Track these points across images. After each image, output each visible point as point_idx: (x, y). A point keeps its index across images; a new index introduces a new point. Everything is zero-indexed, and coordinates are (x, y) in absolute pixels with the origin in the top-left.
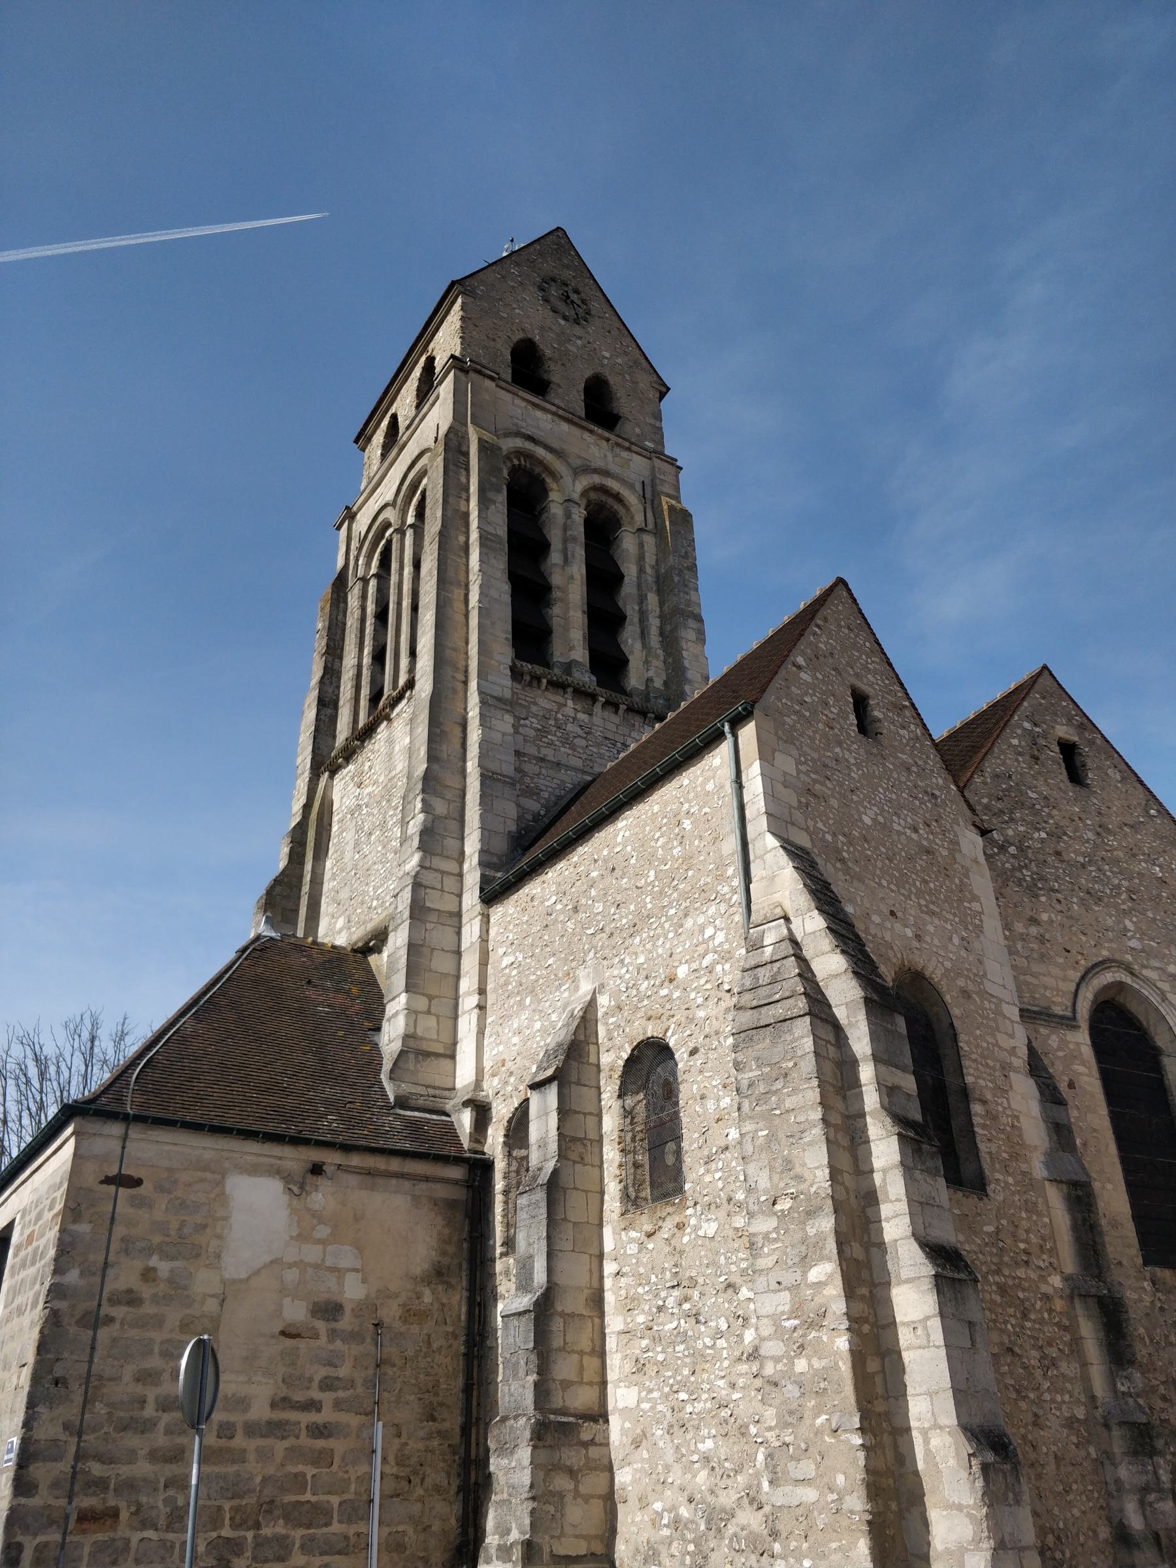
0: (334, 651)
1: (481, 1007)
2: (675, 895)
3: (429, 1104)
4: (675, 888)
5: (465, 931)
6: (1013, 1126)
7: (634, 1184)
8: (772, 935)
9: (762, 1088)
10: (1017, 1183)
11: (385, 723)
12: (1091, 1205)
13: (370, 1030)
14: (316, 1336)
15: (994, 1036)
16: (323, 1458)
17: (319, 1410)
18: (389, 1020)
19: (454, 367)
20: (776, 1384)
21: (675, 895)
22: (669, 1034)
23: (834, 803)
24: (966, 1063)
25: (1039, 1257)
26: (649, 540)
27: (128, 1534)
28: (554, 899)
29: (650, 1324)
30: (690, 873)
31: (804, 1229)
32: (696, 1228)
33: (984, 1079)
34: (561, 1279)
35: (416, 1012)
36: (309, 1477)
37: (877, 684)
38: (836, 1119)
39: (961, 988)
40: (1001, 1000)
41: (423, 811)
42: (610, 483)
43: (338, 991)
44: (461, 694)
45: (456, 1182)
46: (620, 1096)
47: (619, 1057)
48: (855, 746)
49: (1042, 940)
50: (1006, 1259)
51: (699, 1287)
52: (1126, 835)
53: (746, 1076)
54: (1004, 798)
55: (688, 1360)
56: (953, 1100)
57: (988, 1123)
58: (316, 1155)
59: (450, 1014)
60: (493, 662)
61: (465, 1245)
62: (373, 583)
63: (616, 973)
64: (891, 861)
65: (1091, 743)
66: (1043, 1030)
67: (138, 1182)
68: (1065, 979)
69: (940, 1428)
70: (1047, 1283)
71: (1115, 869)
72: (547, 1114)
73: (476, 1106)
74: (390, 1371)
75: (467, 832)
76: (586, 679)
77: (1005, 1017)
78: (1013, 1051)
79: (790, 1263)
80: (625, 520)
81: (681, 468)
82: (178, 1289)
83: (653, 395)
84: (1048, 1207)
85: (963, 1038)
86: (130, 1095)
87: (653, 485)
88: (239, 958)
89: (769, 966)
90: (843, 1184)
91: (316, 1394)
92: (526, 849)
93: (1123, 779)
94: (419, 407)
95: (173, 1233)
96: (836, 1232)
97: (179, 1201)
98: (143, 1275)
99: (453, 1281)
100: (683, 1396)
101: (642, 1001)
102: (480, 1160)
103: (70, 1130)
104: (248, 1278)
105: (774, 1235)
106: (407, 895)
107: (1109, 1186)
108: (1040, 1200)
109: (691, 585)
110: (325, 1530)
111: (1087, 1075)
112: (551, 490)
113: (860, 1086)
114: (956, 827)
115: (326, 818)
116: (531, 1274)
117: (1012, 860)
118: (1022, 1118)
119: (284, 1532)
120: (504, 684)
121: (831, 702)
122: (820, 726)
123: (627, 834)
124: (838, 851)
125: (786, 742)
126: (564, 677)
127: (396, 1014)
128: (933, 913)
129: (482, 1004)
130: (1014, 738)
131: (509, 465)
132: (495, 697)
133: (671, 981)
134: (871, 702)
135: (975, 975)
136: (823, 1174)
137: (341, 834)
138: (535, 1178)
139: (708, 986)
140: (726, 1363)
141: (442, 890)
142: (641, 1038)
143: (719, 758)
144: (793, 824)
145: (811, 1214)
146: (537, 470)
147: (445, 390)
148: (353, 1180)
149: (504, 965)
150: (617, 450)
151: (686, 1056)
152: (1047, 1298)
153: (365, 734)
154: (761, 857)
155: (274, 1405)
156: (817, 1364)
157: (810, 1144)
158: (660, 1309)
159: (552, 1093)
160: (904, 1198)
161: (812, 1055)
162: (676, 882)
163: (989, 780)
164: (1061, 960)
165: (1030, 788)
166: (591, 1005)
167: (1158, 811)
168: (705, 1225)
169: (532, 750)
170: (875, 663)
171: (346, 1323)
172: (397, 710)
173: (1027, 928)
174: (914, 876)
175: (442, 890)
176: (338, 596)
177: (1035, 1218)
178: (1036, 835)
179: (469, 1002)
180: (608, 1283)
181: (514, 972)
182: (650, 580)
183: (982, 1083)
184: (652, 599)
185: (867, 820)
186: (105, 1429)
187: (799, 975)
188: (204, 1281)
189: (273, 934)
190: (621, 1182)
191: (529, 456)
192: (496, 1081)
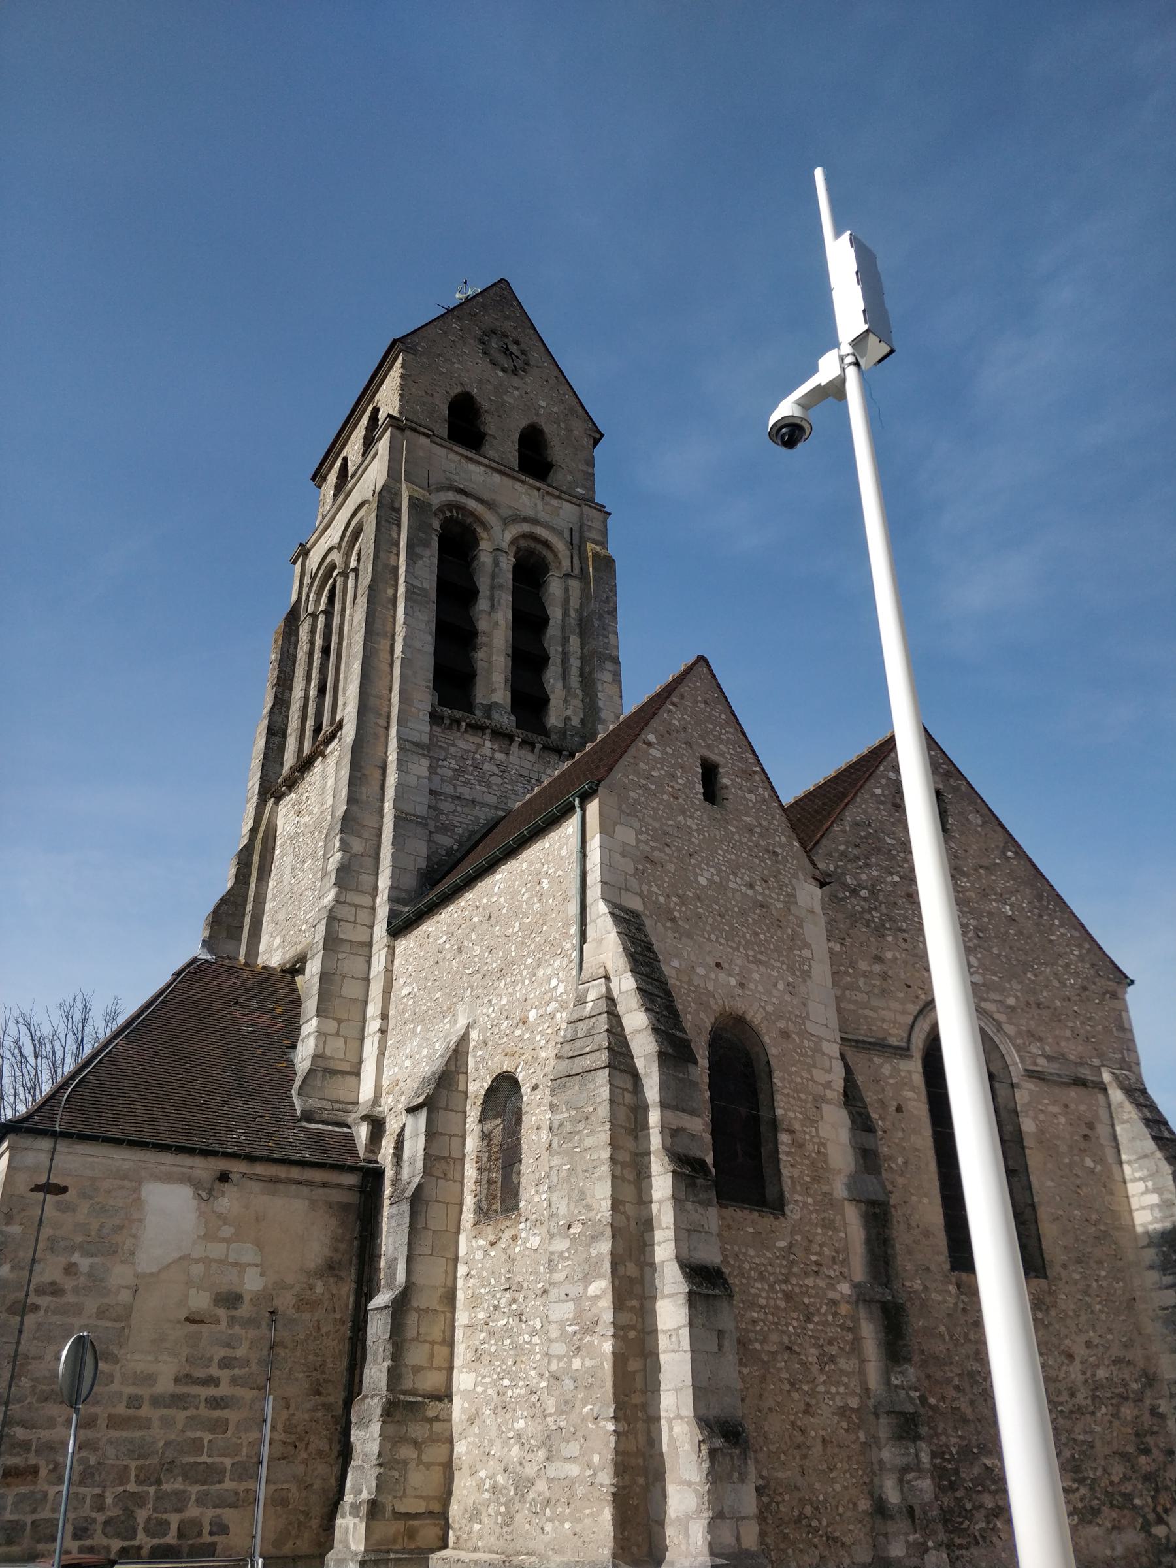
0: (284, 682)
1: (383, 1031)
2: (532, 946)
3: (333, 1118)
4: (533, 941)
5: (374, 959)
6: (819, 1152)
7: (487, 1198)
8: (595, 991)
9: (568, 1129)
10: (815, 1203)
11: (321, 758)
12: (886, 1221)
13: (288, 1047)
14: (217, 1322)
15: (810, 1072)
16: (219, 1426)
17: (217, 1385)
18: (303, 1040)
19: (391, 425)
20: (557, 1379)
21: (532, 946)
22: (519, 1070)
23: (671, 867)
24: (778, 1097)
25: (830, 1268)
26: (574, 585)
27: (46, 1487)
28: (445, 937)
29: (488, 1320)
30: (545, 928)
31: (588, 1251)
32: (526, 1241)
33: (794, 1111)
34: (418, 1279)
35: (325, 1035)
36: (206, 1442)
37: (729, 753)
38: (624, 1157)
39: (781, 1028)
40: (821, 1039)
41: (340, 849)
42: (540, 531)
43: (263, 1010)
44: (382, 739)
45: (350, 1188)
46: (480, 1121)
47: (482, 1087)
48: (699, 813)
49: (884, 976)
50: (795, 1270)
51: (524, 1292)
52: (979, 877)
53: (558, 1117)
54: (862, 845)
55: (511, 1352)
56: (763, 1129)
57: (793, 1150)
58: (223, 1165)
59: (357, 1035)
60: (413, 709)
61: (356, 1243)
62: (322, 618)
63: (485, 1011)
64: (722, 916)
65: (956, 790)
66: (877, 1060)
67: (64, 1190)
68: (904, 1012)
69: (682, 1418)
70: (835, 1290)
71: (965, 909)
72: (417, 1135)
73: (373, 1120)
74: (282, 1352)
75: (381, 868)
76: (505, 719)
77: (824, 1054)
78: (828, 1085)
79: (576, 1278)
80: (553, 565)
81: (610, 514)
82: (96, 1282)
83: (587, 442)
84: (845, 1223)
85: (777, 1074)
86: (60, 1113)
87: (581, 532)
88: (174, 981)
89: (587, 1020)
90: (624, 1213)
91: (214, 1371)
92: (434, 883)
93: (984, 823)
94: (365, 454)
95: (93, 1233)
96: (612, 1254)
97: (100, 1206)
98: (65, 1269)
99: (343, 1274)
100: (506, 1382)
101: (500, 1038)
102: (373, 1168)
103: (5, 1145)
104: (159, 1271)
105: (567, 1255)
106: (322, 927)
107: (925, 1200)
108: (838, 1217)
109: (610, 629)
110: (218, 1487)
111: (915, 1100)
112: (482, 539)
113: (648, 1128)
114: (794, 881)
115: (270, 839)
116: (395, 1274)
117: (863, 903)
118: (829, 1145)
119: (182, 1487)
120: (422, 729)
121: (679, 774)
122: (665, 797)
123: (502, 886)
124: (670, 911)
125: (628, 815)
126: (482, 720)
127: (308, 1036)
128: (760, 962)
129: (384, 1028)
130: (878, 788)
131: (441, 517)
132: (413, 743)
133: (524, 1023)
134: (721, 770)
135: (797, 1016)
136: (606, 1205)
137: (283, 858)
138: (404, 1191)
139: (549, 1031)
140: (538, 1357)
141: (355, 923)
142: (499, 1071)
143: (570, 828)
144: (627, 890)
145: (594, 1238)
146: (469, 521)
147: (383, 446)
148: (256, 1187)
149: (403, 995)
150: (548, 498)
151: (529, 1090)
152: (833, 1303)
153: (305, 765)
154: (595, 921)
155: (177, 1380)
156: (588, 1363)
157: (600, 1178)
158: (496, 1308)
159: (423, 1116)
160: (672, 1227)
161: (608, 1102)
162: (534, 935)
163: (848, 828)
164: (901, 995)
165: (888, 835)
166: (464, 1038)
167: (1016, 853)
168: (532, 1239)
169: (449, 789)
170: (729, 733)
171: (245, 1310)
172: (331, 747)
173: (870, 966)
174: (744, 929)
175: (355, 923)
176: (290, 629)
177: (830, 1233)
178: (889, 879)
179: (373, 1026)
180: (460, 1283)
181: (411, 1002)
182: (573, 622)
183: (791, 1114)
184: (575, 641)
185: (703, 881)
186: (29, 1400)
187: (607, 1030)
188: (119, 1275)
189: (208, 957)
190: (475, 1196)
191: (461, 508)
192: (391, 1098)
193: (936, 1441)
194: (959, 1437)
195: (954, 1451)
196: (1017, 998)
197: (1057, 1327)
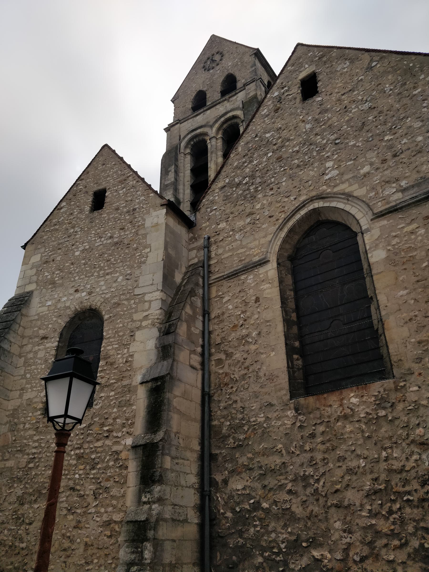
193: (265, 538)
194: (289, 533)
195: (283, 546)
196: (371, 164)
197: (405, 419)
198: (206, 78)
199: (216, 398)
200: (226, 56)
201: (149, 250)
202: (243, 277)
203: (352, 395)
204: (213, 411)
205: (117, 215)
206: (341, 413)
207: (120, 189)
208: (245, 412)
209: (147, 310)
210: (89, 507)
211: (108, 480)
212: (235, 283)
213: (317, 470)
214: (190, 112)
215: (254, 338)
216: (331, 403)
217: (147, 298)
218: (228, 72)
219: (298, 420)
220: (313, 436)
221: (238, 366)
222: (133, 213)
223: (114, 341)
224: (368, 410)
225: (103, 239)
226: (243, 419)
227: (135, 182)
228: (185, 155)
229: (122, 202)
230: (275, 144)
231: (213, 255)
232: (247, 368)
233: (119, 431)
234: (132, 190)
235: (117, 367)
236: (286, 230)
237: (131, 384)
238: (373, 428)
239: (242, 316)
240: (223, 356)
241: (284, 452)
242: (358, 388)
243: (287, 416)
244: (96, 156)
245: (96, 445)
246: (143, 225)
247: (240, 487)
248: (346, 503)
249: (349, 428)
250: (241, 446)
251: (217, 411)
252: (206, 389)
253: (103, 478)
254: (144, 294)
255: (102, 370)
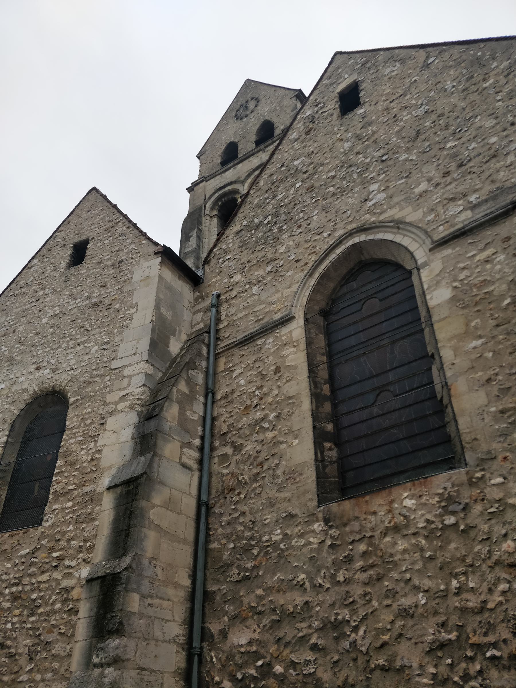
196: (429, 180)
197: (485, 527)
198: (238, 127)
199: (217, 510)
200: (263, 101)
201: (135, 310)
202: (259, 342)
203: (406, 494)
204: (212, 529)
205: (99, 270)
206: (390, 523)
207: (105, 239)
208: (256, 529)
209: (125, 389)
210: (21, 673)
211: (50, 631)
212: (250, 350)
213: (354, 612)
214: (220, 167)
215: (272, 422)
216: (375, 509)
217: (126, 372)
218: (265, 119)
219: (329, 537)
220: (349, 559)
221: (249, 463)
222: (119, 266)
223: (79, 432)
224: (429, 517)
225: (78, 301)
226: (252, 538)
227: (124, 228)
228: (211, 217)
229: (107, 254)
230: (306, 172)
231: (223, 316)
232: (261, 464)
233: (72, 557)
234: (120, 238)
235: (79, 467)
236: (317, 275)
237: (95, 491)
238: (437, 543)
239: (257, 393)
240: (229, 450)
241: (307, 584)
242: (414, 485)
243: (313, 531)
244: (81, 202)
245: (39, 579)
246: (130, 279)
247: (243, 641)
248: (398, 663)
249: (402, 545)
250: (248, 578)
251: (217, 529)
252: (204, 498)
253: (43, 629)
254: (123, 367)
255: (58, 473)
